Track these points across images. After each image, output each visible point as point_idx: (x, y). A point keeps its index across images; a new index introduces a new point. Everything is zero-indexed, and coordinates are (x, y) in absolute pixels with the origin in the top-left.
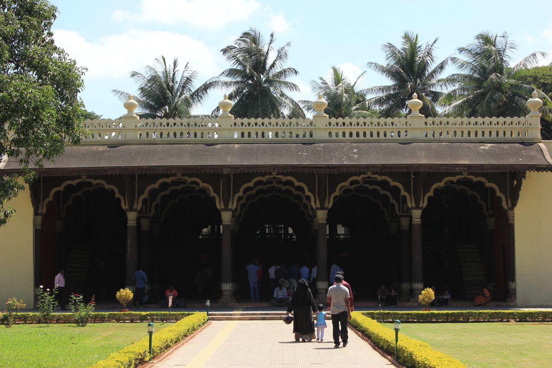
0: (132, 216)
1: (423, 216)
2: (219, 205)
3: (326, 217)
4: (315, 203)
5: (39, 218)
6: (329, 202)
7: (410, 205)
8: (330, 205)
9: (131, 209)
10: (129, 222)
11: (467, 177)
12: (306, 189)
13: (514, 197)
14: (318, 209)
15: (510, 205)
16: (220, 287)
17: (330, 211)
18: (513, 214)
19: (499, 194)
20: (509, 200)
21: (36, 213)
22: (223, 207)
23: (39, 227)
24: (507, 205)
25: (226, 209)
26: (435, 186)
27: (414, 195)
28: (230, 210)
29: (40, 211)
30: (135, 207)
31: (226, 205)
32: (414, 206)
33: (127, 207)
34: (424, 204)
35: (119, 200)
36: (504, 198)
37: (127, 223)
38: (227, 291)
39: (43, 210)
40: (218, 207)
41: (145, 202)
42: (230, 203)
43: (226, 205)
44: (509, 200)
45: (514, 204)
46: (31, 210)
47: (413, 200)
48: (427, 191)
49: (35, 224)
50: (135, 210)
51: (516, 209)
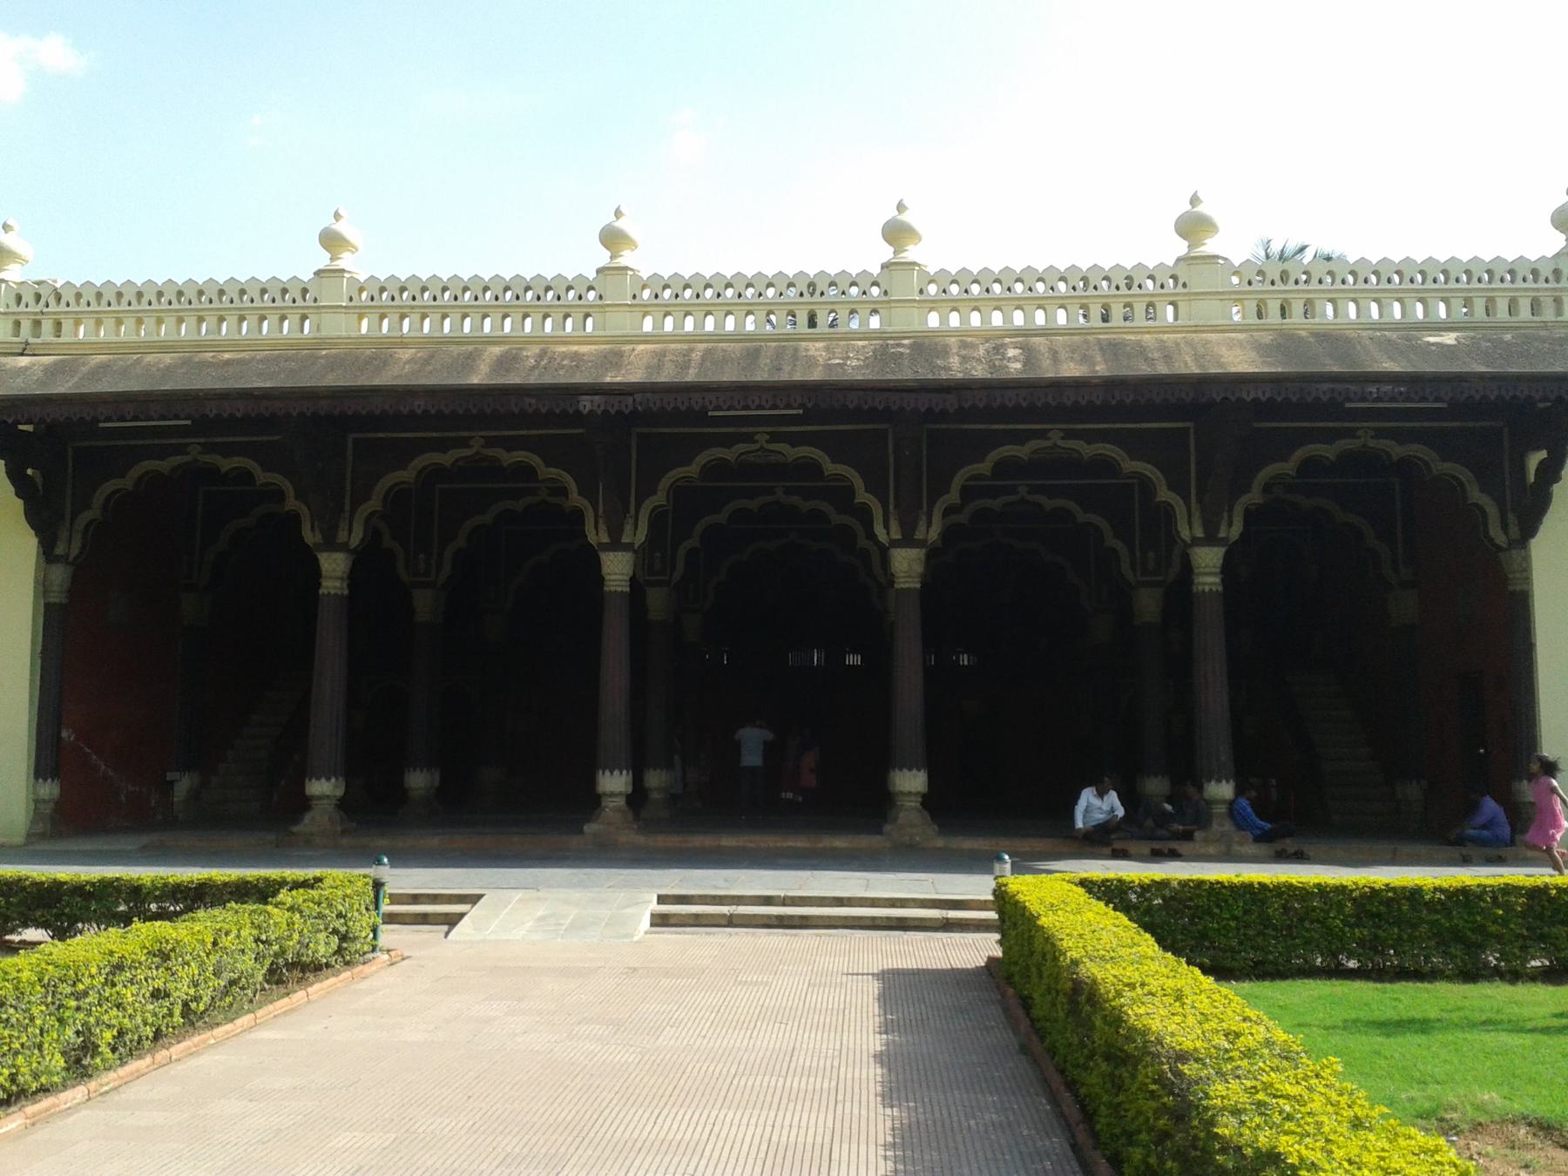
0: (334, 568)
1: (1227, 569)
2: (596, 535)
4: (887, 526)
5: (60, 575)
7: (1185, 534)
9: (331, 544)
10: (325, 583)
11: (1372, 443)
12: (859, 484)
14: (895, 544)
15: (1514, 531)
16: (592, 782)
17: (933, 555)
18: (1527, 559)
19: (1476, 495)
20: (1511, 517)
21: (48, 552)
22: (605, 539)
23: (55, 598)
24: (1506, 533)
25: (616, 545)
27: (1200, 501)
28: (628, 547)
29: (60, 550)
30: (342, 536)
31: (615, 532)
32: (1199, 533)
33: (318, 538)
34: (1234, 530)
38: (612, 794)
39: (71, 545)
40: (592, 538)
41: (657, 519)
42: (628, 528)
43: (615, 532)
44: (1511, 517)
47: (1196, 515)
49: (43, 586)
50: (343, 547)
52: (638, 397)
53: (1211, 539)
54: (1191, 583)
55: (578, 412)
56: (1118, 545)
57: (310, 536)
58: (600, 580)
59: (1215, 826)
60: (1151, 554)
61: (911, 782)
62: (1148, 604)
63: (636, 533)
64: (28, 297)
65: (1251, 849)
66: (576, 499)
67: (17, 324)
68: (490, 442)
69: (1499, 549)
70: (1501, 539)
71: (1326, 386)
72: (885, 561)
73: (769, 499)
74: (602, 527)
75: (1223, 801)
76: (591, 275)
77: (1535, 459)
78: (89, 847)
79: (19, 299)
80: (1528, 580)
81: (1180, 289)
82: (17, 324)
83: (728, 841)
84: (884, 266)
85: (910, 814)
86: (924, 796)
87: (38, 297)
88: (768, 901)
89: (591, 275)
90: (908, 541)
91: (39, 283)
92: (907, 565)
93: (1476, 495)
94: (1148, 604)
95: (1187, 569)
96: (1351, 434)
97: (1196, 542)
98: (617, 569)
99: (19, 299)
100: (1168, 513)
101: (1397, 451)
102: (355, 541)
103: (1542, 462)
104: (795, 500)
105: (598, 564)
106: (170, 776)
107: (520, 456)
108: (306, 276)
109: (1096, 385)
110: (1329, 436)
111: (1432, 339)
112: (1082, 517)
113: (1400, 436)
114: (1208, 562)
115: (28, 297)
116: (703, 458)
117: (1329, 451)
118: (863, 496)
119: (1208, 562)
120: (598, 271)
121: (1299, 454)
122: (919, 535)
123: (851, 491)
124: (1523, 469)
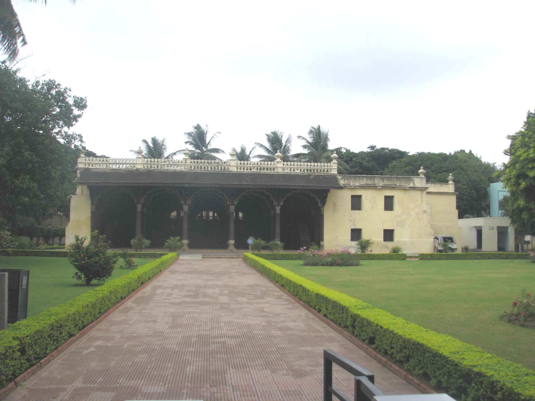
0: (139, 207)
1: (281, 210)
13: (324, 202)
21: (92, 204)
45: (324, 205)
46: (90, 202)
49: (91, 209)
51: (325, 207)
53: (278, 205)
61: (232, 242)
63: (189, 202)
70: (320, 205)
72: (229, 208)
85: (232, 247)
95: (275, 210)
108: (135, 158)
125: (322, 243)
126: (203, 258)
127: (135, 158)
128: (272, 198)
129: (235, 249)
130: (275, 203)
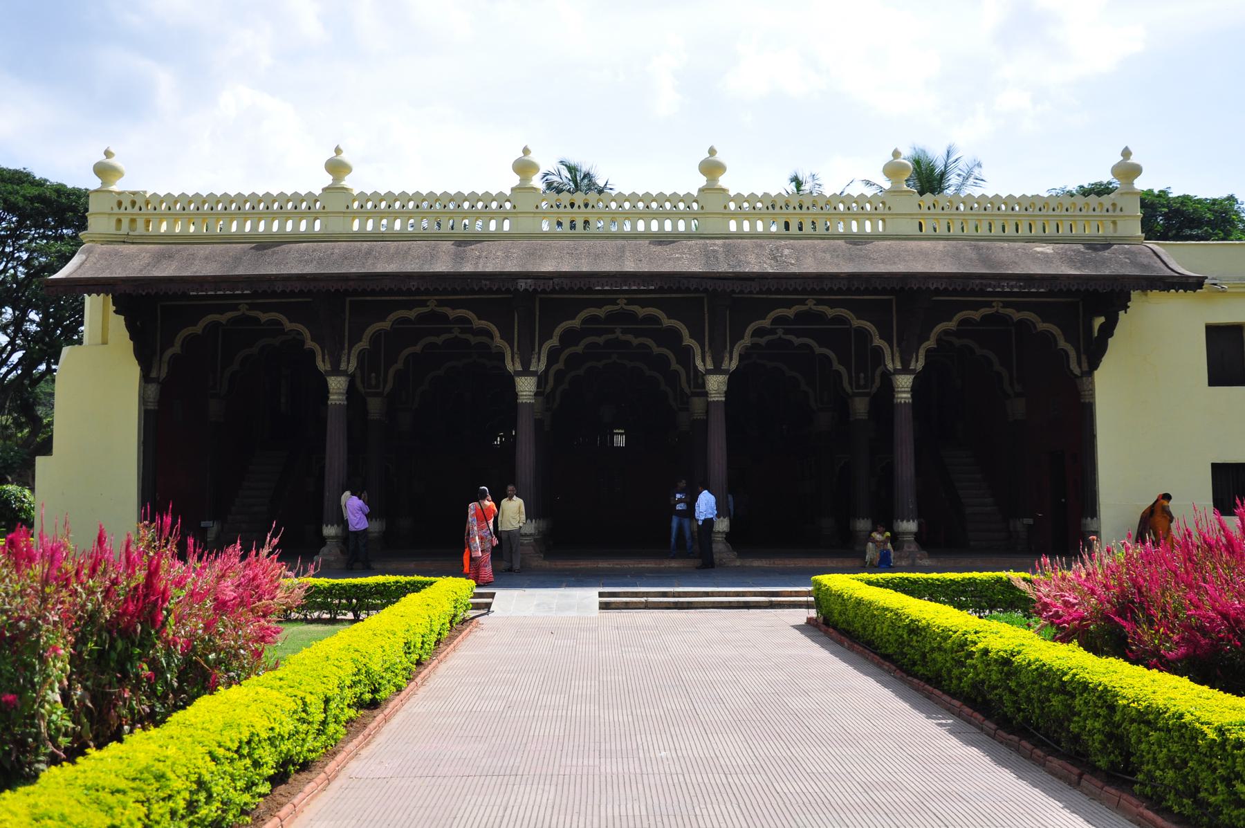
0: (337, 385)
1: (914, 390)
3: (725, 389)
4: (704, 361)
5: (153, 389)
6: (731, 359)
7: (890, 367)
8: (734, 365)
11: (1001, 311)
12: (685, 332)
13: (1095, 352)
14: (709, 372)
15: (1085, 366)
17: (734, 380)
18: (1092, 383)
19: (1062, 344)
20: (1084, 358)
21: (146, 378)
23: (151, 407)
24: (1080, 367)
25: (526, 372)
26: (939, 328)
27: (899, 345)
29: (154, 375)
30: (343, 366)
31: (526, 365)
32: (899, 367)
33: (328, 367)
34: (919, 364)
35: (312, 353)
36: (1073, 354)
37: (328, 398)
40: (510, 367)
42: (534, 361)
43: (526, 365)
45: (1094, 365)
47: (897, 355)
48: (924, 338)
49: (143, 399)
50: (344, 373)
51: (1098, 374)
52: (556, 280)
54: (893, 396)
55: (517, 290)
56: (842, 369)
57: (322, 366)
58: (515, 395)
59: (906, 549)
60: (862, 375)
62: (861, 406)
63: (539, 365)
64: (126, 203)
65: (927, 562)
66: (498, 341)
67: (119, 221)
68: (441, 303)
69: (1076, 376)
70: (1077, 371)
71: (978, 281)
72: (703, 385)
73: (611, 336)
74: (517, 361)
75: (910, 533)
76: (508, 192)
77: (1099, 321)
78: (840, 565)
79: (120, 204)
80: (1093, 395)
81: (887, 211)
82: (119, 221)
83: (603, 564)
84: (701, 190)
86: (727, 534)
87: (133, 203)
88: (665, 594)
89: (508, 192)
90: (717, 370)
91: (134, 193)
92: (716, 385)
93: (1062, 344)
94: (861, 406)
96: (989, 304)
97: (897, 372)
98: (526, 387)
99: (120, 204)
100: (878, 352)
101: (1017, 316)
102: (351, 369)
103: (1101, 326)
104: (629, 337)
105: (513, 385)
106: (203, 524)
107: (461, 312)
108: (318, 192)
109: (843, 278)
110: (976, 306)
111: (1039, 249)
112: (819, 350)
113: (1019, 307)
114: (904, 383)
115: (126, 203)
116: (584, 314)
117: (976, 315)
118: (688, 341)
119: (904, 383)
120: (512, 189)
121: (958, 317)
122: (724, 367)
123: (679, 337)
124: (1091, 328)
125: (1090, 523)
126: (604, 606)
127: (318, 192)
128: (878, 342)
129: (733, 555)
130: (891, 363)
